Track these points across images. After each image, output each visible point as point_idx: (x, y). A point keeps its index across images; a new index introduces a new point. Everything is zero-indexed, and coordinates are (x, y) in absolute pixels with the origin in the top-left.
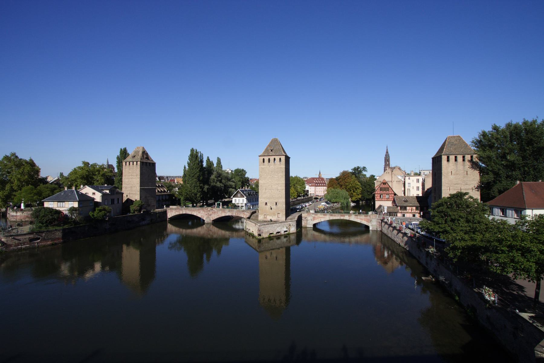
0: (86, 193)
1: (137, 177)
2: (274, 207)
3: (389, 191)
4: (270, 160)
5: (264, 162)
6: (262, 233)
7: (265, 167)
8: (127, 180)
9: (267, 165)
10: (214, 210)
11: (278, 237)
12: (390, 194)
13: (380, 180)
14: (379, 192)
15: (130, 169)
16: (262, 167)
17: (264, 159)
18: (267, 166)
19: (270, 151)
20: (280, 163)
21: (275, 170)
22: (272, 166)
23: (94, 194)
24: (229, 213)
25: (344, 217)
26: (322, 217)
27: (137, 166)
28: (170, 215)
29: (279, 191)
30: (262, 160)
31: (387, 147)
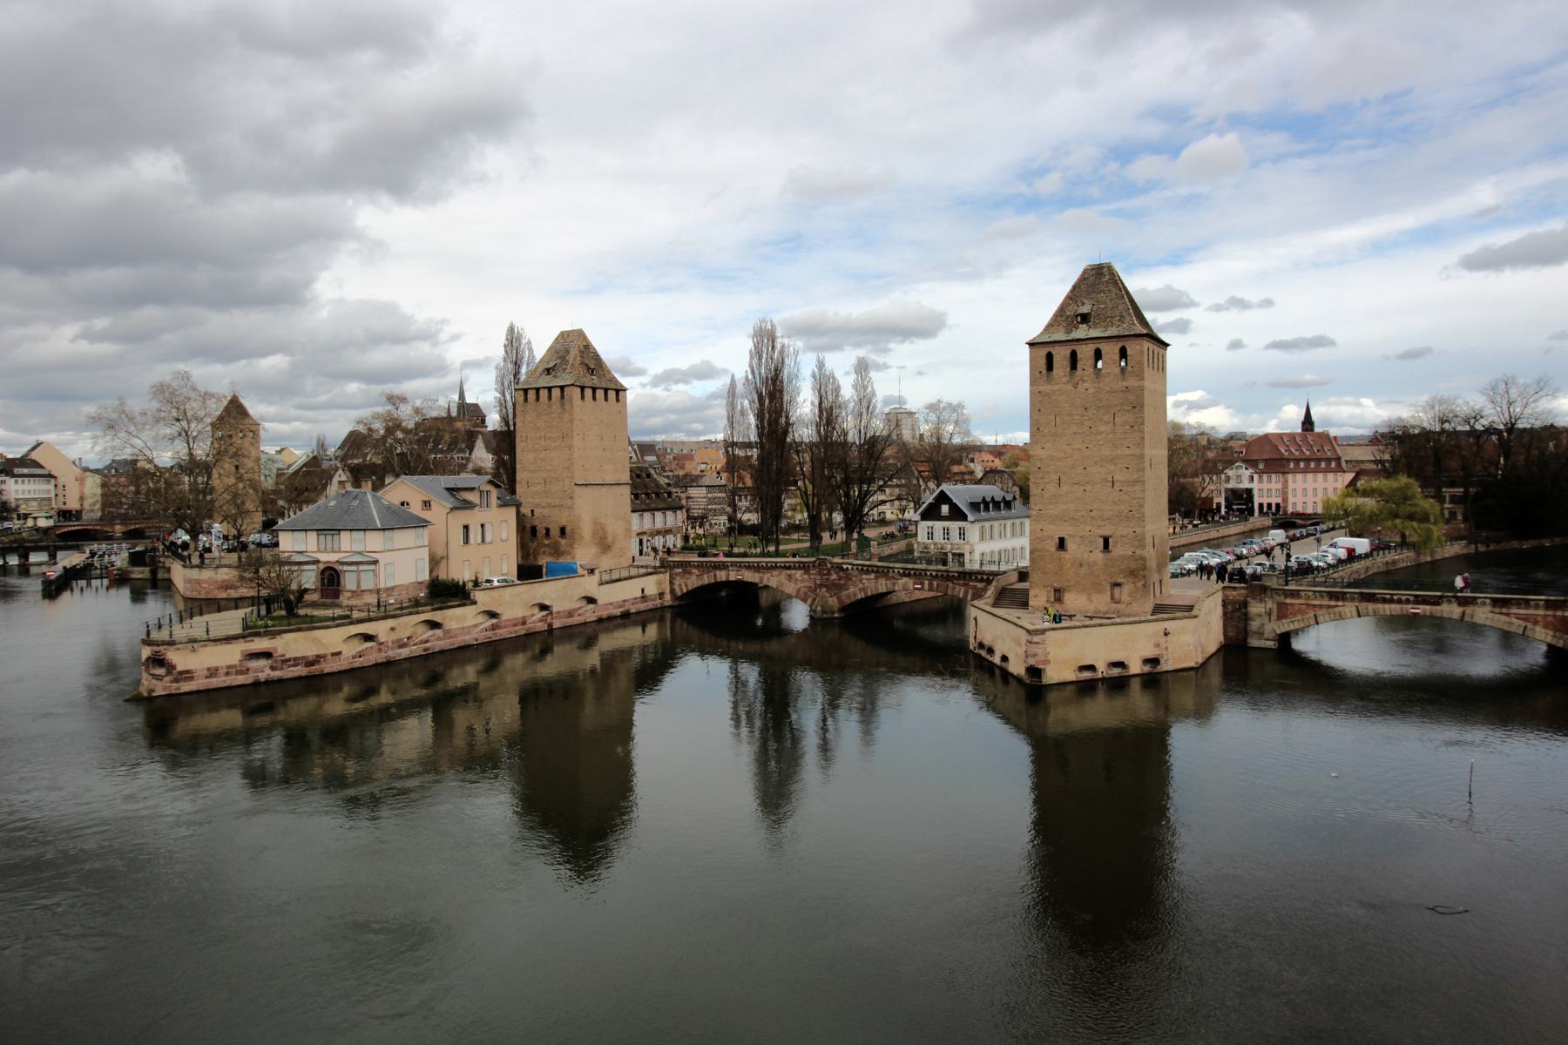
0: (403, 504)
2: (1098, 556)
5: (1050, 367)
6: (1047, 662)
7: (1055, 388)
8: (531, 456)
9: (1064, 380)
11: (1118, 684)
16: (1042, 388)
17: (1050, 357)
18: (1065, 383)
19: (1079, 319)
22: (1085, 385)
23: (427, 504)
25: (1434, 607)
26: (1321, 606)
27: (563, 405)
28: (680, 585)
29: (1117, 487)
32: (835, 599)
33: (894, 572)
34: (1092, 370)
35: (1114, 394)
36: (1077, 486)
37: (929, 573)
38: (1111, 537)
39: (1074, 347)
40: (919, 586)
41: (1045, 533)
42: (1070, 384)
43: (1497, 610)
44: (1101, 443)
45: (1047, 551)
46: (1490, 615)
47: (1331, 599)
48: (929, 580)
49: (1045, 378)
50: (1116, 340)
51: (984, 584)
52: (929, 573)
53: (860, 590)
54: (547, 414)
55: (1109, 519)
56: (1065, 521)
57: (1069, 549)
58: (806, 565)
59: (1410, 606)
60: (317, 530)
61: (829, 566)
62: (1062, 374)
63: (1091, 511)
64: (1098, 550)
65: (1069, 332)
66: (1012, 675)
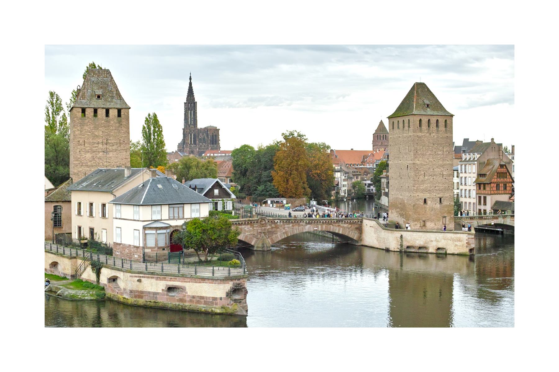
1: (119, 148)
2: (438, 205)
3: (506, 178)
4: (431, 122)
7: (423, 134)
8: (89, 156)
9: (426, 131)
10: (276, 221)
12: (508, 182)
13: (482, 160)
14: (495, 180)
15: (96, 128)
17: (420, 120)
19: (426, 106)
20: (446, 130)
21: (438, 141)
24: (310, 225)
25: (497, 220)
30: (419, 123)
31: (190, 79)
32: (269, 240)
33: (303, 222)
34: (436, 128)
35: (443, 139)
36: (430, 177)
37: (322, 222)
38: (442, 197)
39: (430, 118)
40: (317, 229)
41: (419, 197)
42: (428, 133)
43: (512, 219)
44: (439, 159)
45: (421, 205)
46: (510, 221)
47: (470, 220)
48: (321, 225)
49: (419, 130)
50: (443, 117)
51: (348, 225)
52: (322, 222)
53: (283, 233)
54: (105, 127)
55: (441, 190)
56: (427, 191)
57: (428, 203)
58: (253, 222)
59: (491, 220)
60: (169, 204)
61: (267, 221)
62: (425, 129)
63: (436, 187)
64: (438, 204)
65: (425, 111)
66: (453, 254)
